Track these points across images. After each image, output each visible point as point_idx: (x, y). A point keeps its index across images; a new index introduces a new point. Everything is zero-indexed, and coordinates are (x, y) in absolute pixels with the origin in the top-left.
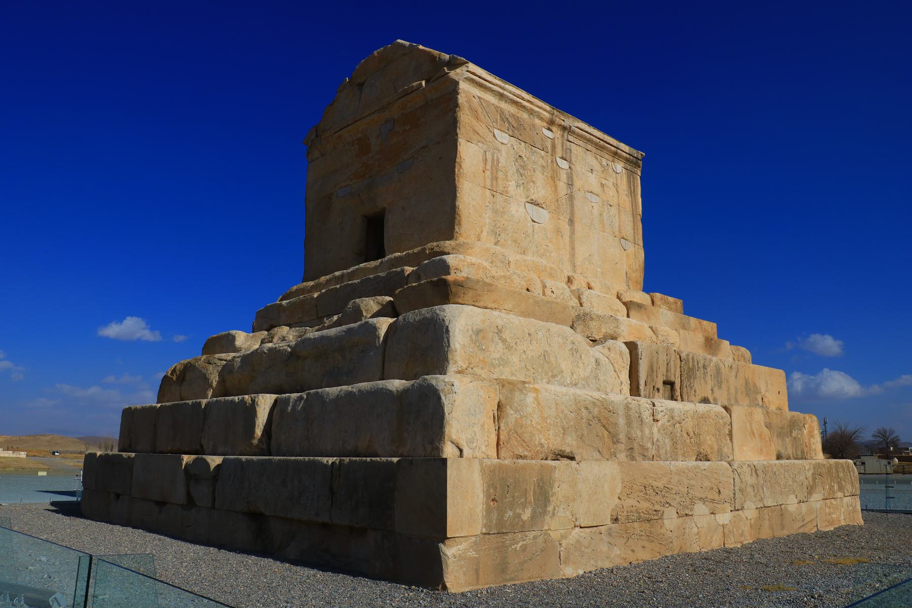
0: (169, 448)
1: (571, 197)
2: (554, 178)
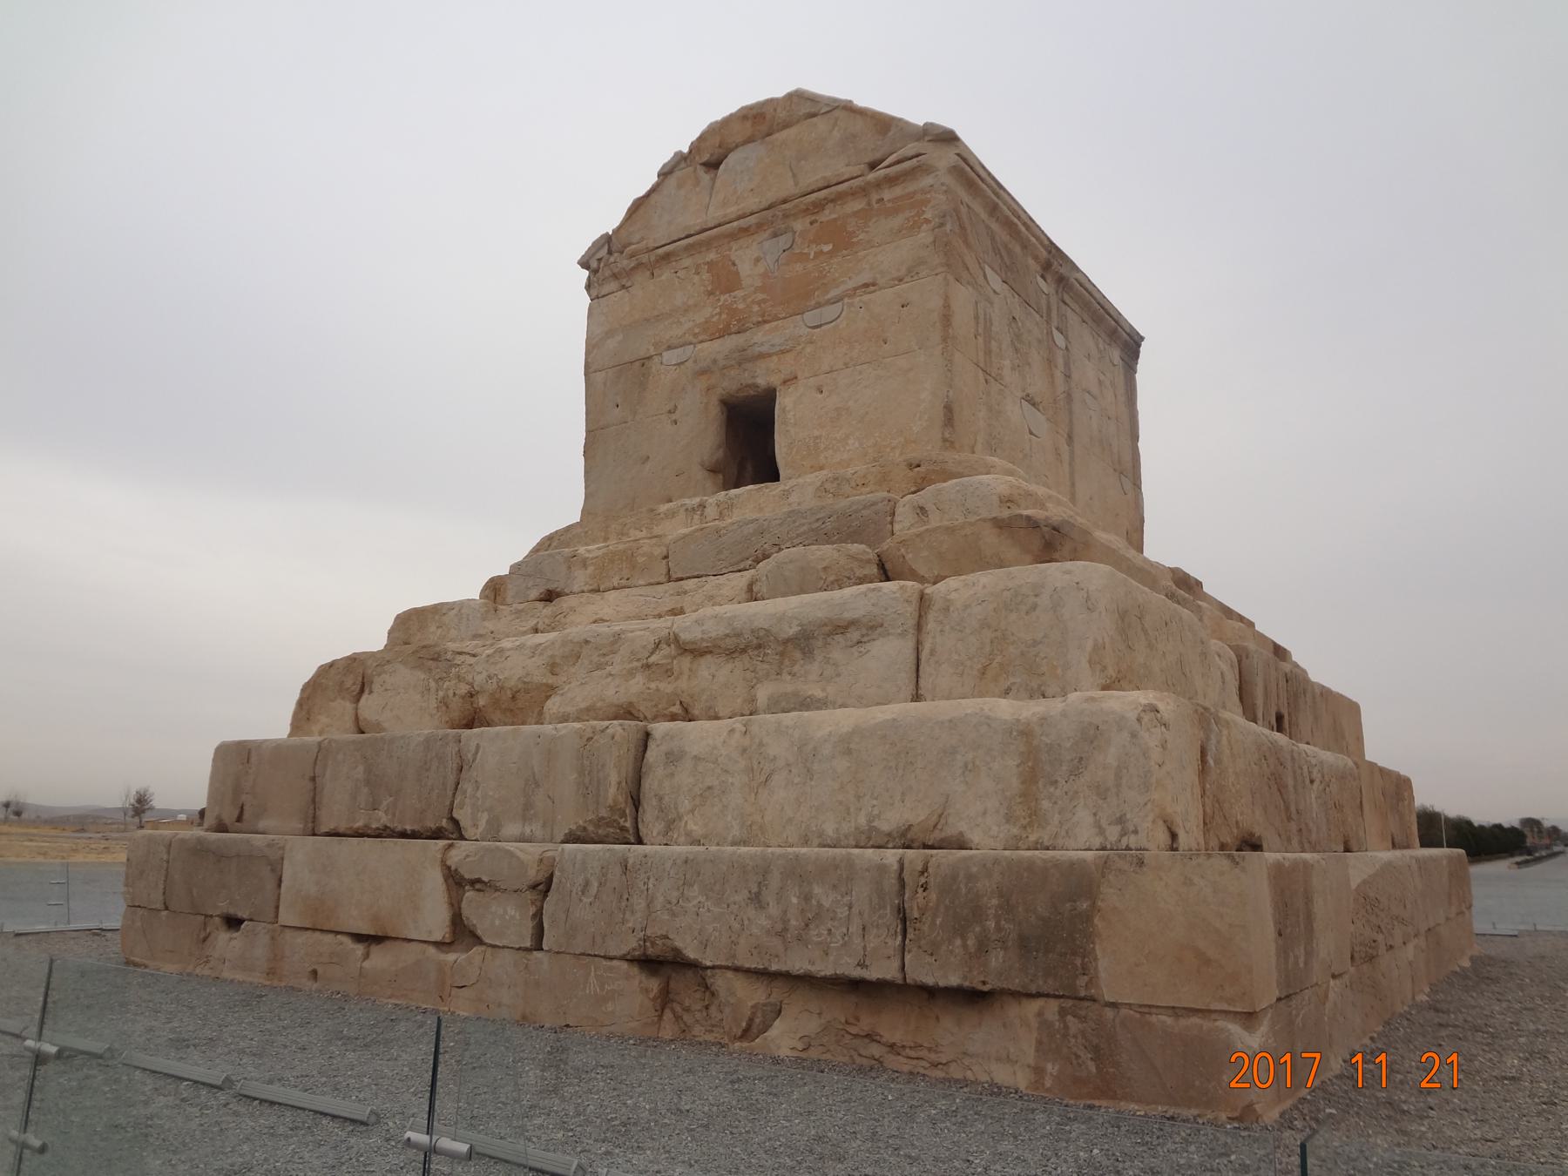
0: (359, 824)
1: (1069, 397)
2: (1050, 362)
